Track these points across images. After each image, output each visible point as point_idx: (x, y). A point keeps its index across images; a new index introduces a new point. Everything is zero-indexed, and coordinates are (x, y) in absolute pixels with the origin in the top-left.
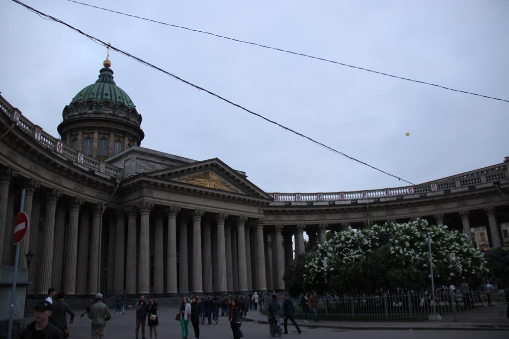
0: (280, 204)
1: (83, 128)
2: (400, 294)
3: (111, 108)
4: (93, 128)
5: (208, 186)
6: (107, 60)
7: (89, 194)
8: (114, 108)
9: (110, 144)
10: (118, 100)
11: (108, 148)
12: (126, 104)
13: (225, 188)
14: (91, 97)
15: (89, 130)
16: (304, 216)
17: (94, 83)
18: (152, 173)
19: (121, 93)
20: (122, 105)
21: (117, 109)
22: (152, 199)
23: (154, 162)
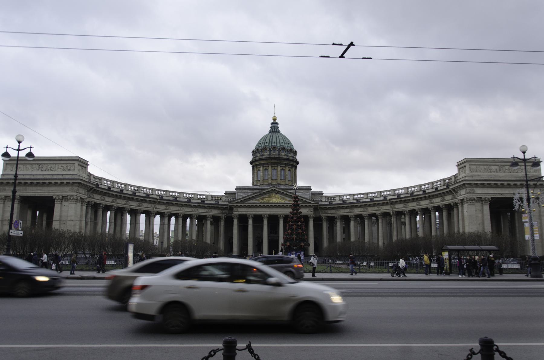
0: (339, 202)
1: (257, 165)
2: (377, 262)
3: (268, 151)
4: (259, 165)
5: (271, 202)
6: (275, 117)
7: (215, 212)
8: (270, 150)
9: (269, 172)
10: (273, 144)
11: (268, 175)
12: (278, 145)
13: (283, 202)
14: (259, 146)
15: (266, 165)
16: (354, 209)
17: (268, 133)
18: (234, 201)
19: (276, 139)
20: (274, 147)
21: (272, 150)
22: (238, 212)
23: (248, 192)
